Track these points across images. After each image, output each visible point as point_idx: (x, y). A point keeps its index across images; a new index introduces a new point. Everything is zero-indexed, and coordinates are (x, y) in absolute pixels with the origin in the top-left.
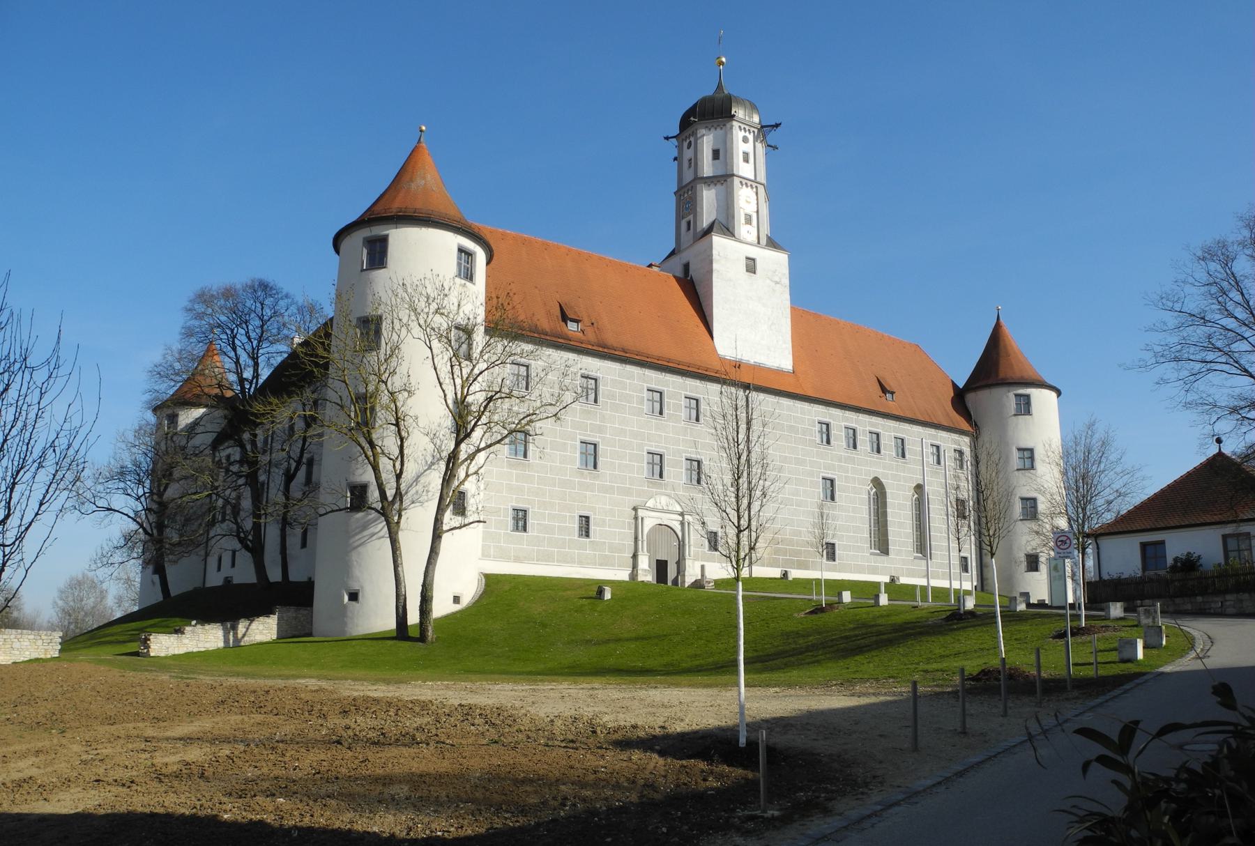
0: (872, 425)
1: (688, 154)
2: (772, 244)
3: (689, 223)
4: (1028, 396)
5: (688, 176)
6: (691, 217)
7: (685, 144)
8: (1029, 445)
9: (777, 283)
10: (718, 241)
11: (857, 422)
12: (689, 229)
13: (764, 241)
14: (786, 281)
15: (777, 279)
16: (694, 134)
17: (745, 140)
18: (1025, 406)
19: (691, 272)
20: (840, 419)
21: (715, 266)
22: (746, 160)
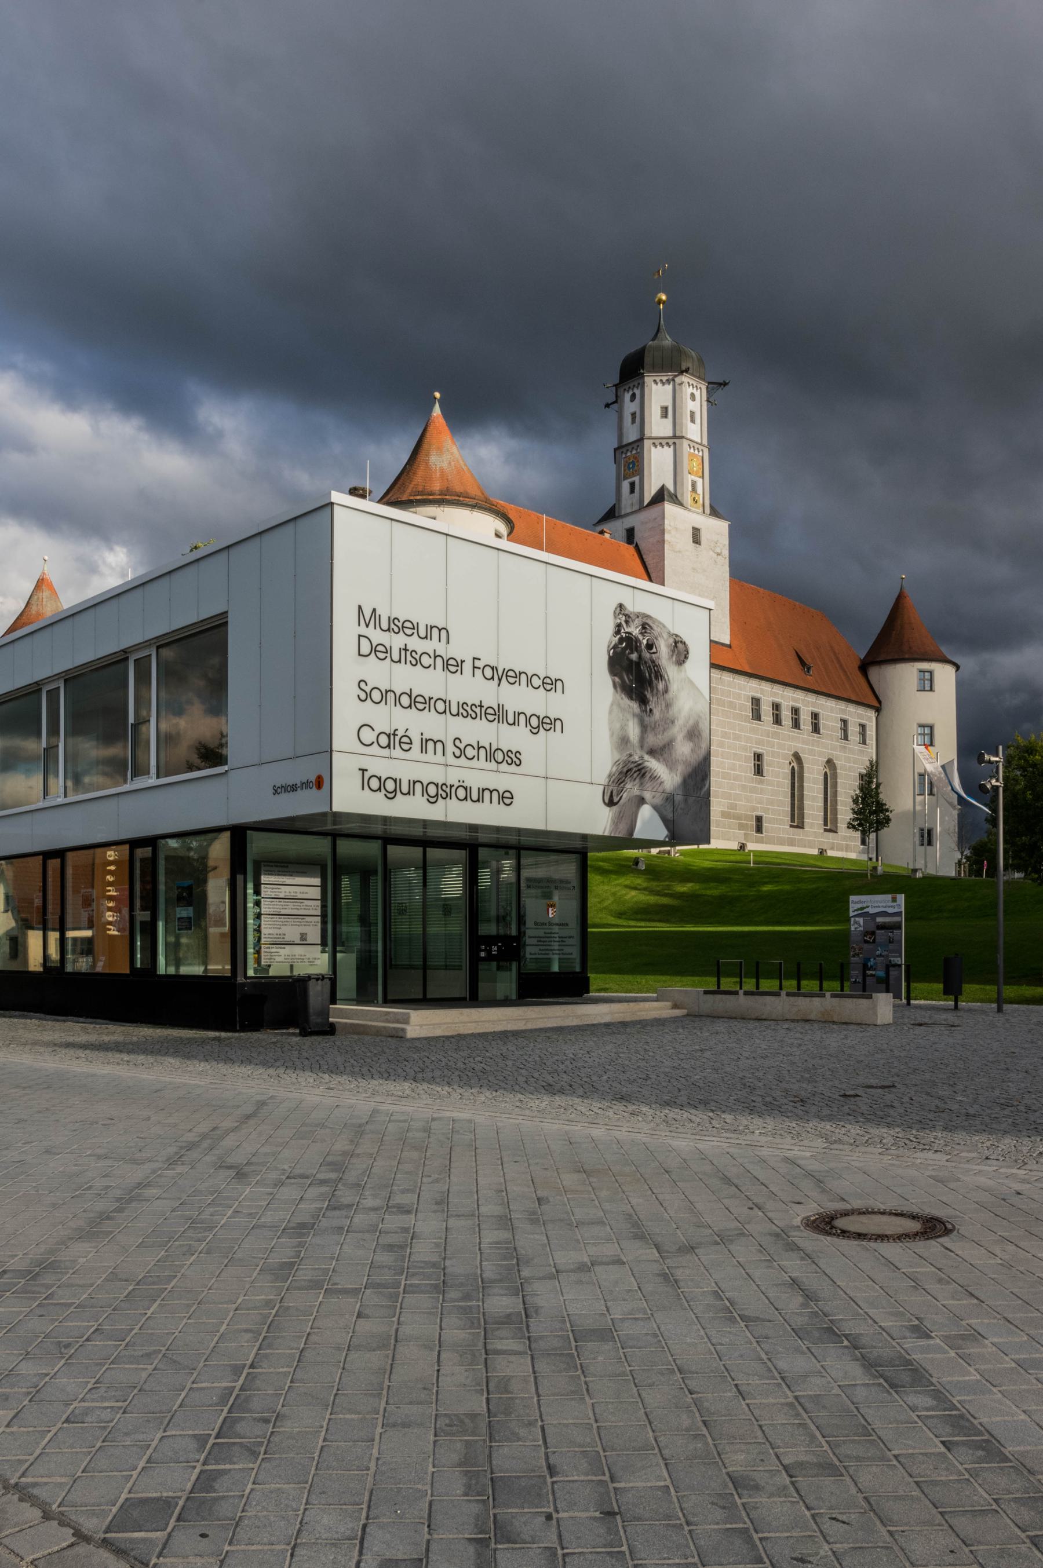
0: (795, 700)
1: (630, 408)
2: (714, 513)
3: (632, 485)
4: (931, 673)
5: (631, 436)
6: (636, 479)
7: (627, 396)
8: (929, 721)
9: (718, 554)
10: (669, 508)
11: (782, 697)
12: (632, 491)
13: (708, 510)
14: (726, 552)
15: (718, 550)
16: (642, 385)
17: (693, 397)
18: (927, 684)
19: (636, 539)
20: (769, 693)
21: (667, 537)
22: (693, 421)
